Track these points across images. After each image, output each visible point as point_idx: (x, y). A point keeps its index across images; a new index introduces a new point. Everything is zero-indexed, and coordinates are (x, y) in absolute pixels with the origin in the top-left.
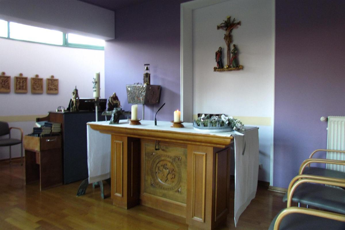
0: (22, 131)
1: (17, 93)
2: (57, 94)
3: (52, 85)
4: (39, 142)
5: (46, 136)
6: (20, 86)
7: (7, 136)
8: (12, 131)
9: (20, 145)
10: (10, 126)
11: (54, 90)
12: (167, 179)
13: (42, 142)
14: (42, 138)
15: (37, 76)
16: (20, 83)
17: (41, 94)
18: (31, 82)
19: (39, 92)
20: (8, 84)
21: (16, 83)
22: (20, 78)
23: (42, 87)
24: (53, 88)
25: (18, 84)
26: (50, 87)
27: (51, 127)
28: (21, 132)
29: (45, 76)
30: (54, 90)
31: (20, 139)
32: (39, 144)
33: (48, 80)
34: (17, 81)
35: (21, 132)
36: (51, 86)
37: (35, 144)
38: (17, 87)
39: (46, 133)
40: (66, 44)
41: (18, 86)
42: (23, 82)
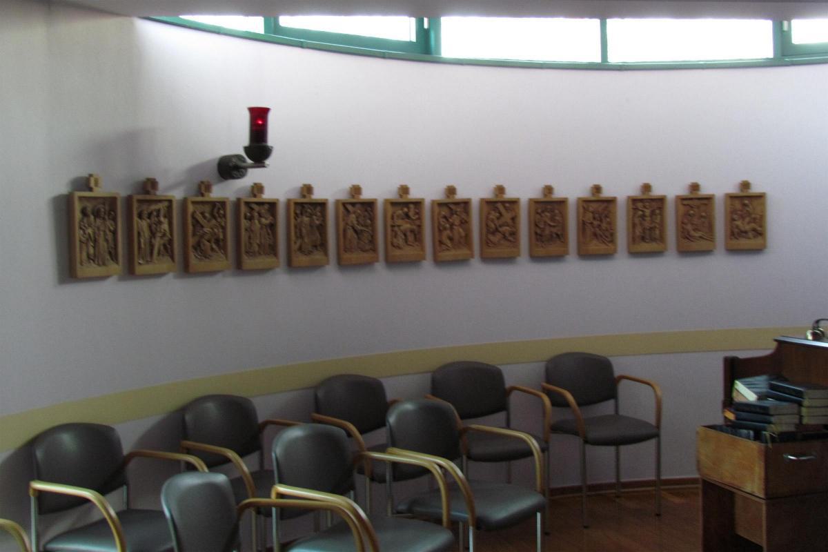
0: (659, 393)
1: (634, 254)
2: (759, 250)
3: (742, 217)
4: (763, 464)
5: (785, 438)
6: (644, 230)
7: (607, 408)
8: (624, 388)
9: (653, 442)
10: (617, 372)
11: (750, 234)
12: (394, 246)
13: (771, 462)
14: (770, 445)
15: (695, 187)
16: (643, 217)
17: (707, 252)
18: (677, 211)
19: (703, 245)
20: (610, 223)
21: (633, 220)
22: (641, 200)
23: (711, 228)
24: (747, 227)
25: (637, 221)
26: (737, 227)
27: (800, 404)
28: (656, 396)
29: (719, 186)
30: (750, 234)
31: (652, 420)
32: (759, 470)
33: (732, 197)
34: (636, 209)
35: (656, 396)
36: (739, 223)
37: (744, 469)
38: (634, 232)
39: (784, 429)
40: (787, 54)
41: (638, 231)
42: (653, 213)
